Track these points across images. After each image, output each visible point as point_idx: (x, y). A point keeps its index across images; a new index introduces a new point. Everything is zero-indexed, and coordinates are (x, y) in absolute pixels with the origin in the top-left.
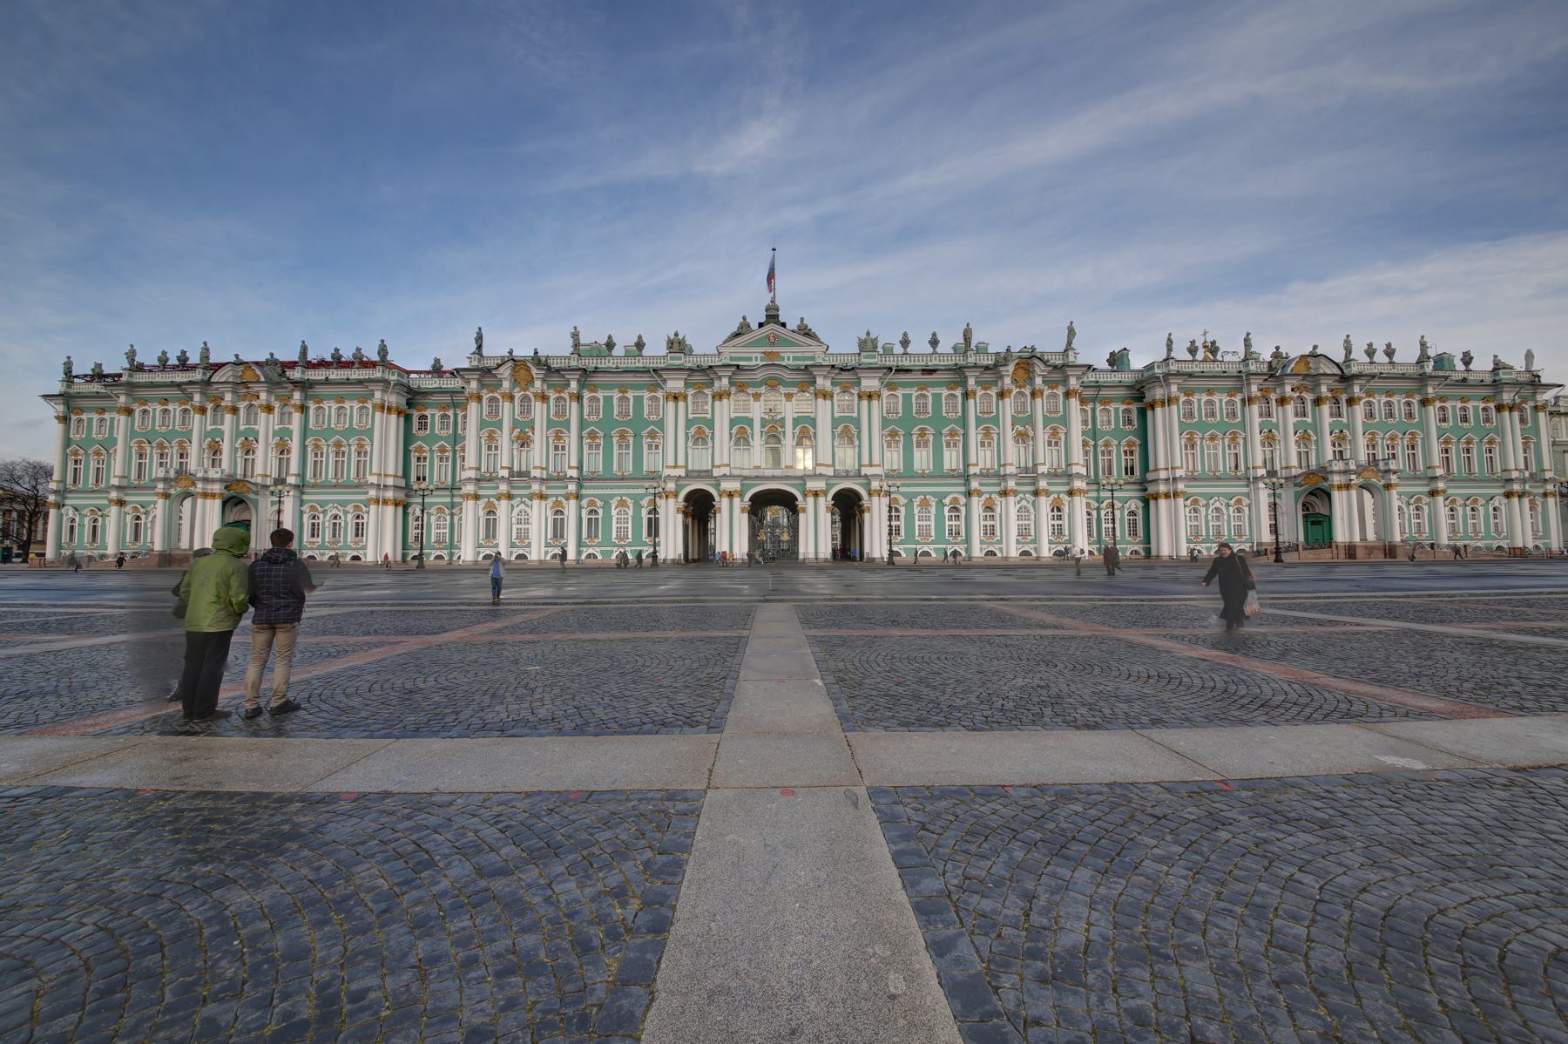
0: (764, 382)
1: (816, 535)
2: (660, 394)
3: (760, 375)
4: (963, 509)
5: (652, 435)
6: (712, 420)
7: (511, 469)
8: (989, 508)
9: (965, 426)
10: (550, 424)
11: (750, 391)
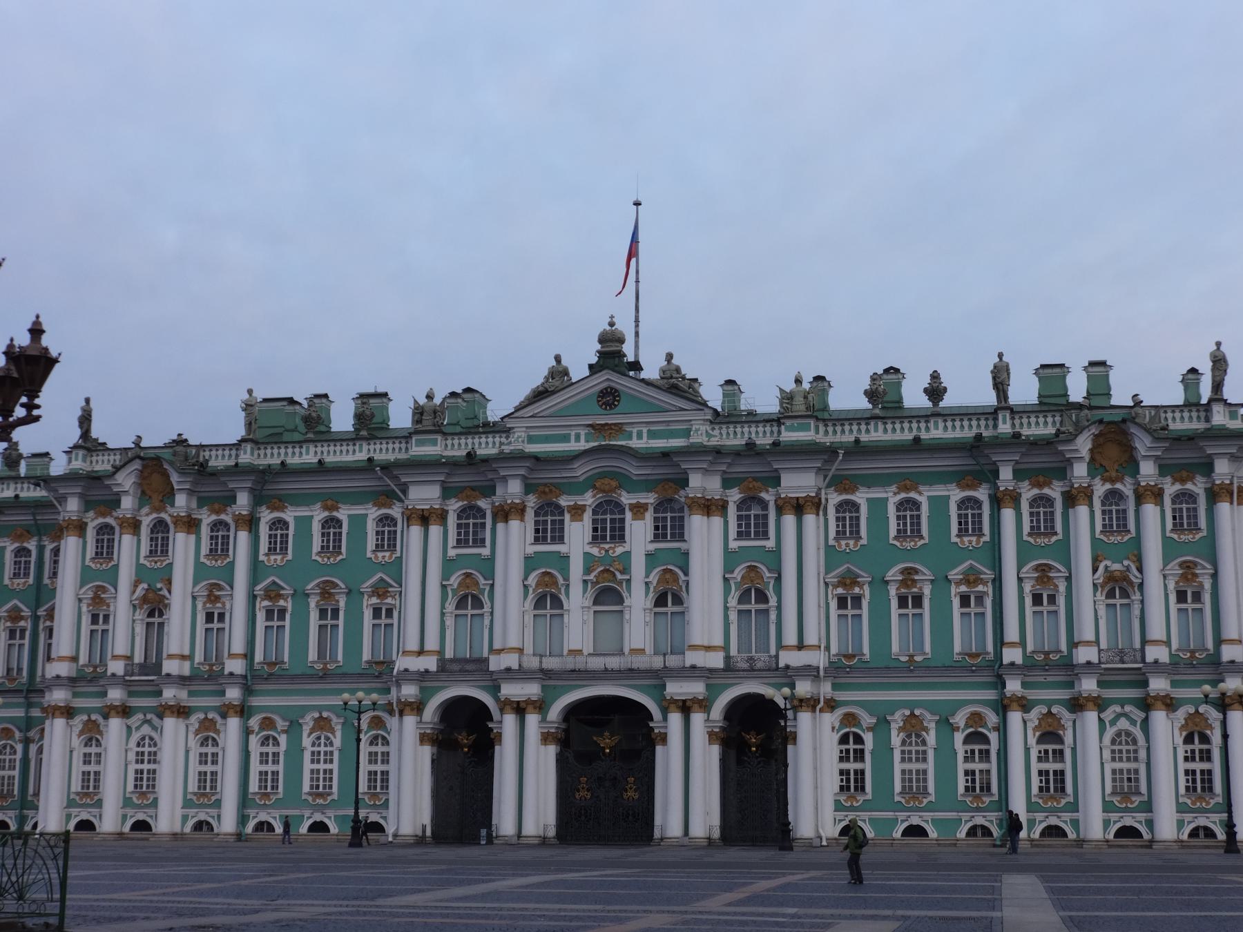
0: (591, 483)
1: (688, 787)
2: (396, 511)
3: (581, 471)
4: (993, 737)
5: (380, 590)
6: (491, 559)
7: (129, 658)
8: (1050, 734)
10: (200, 571)
11: (564, 501)
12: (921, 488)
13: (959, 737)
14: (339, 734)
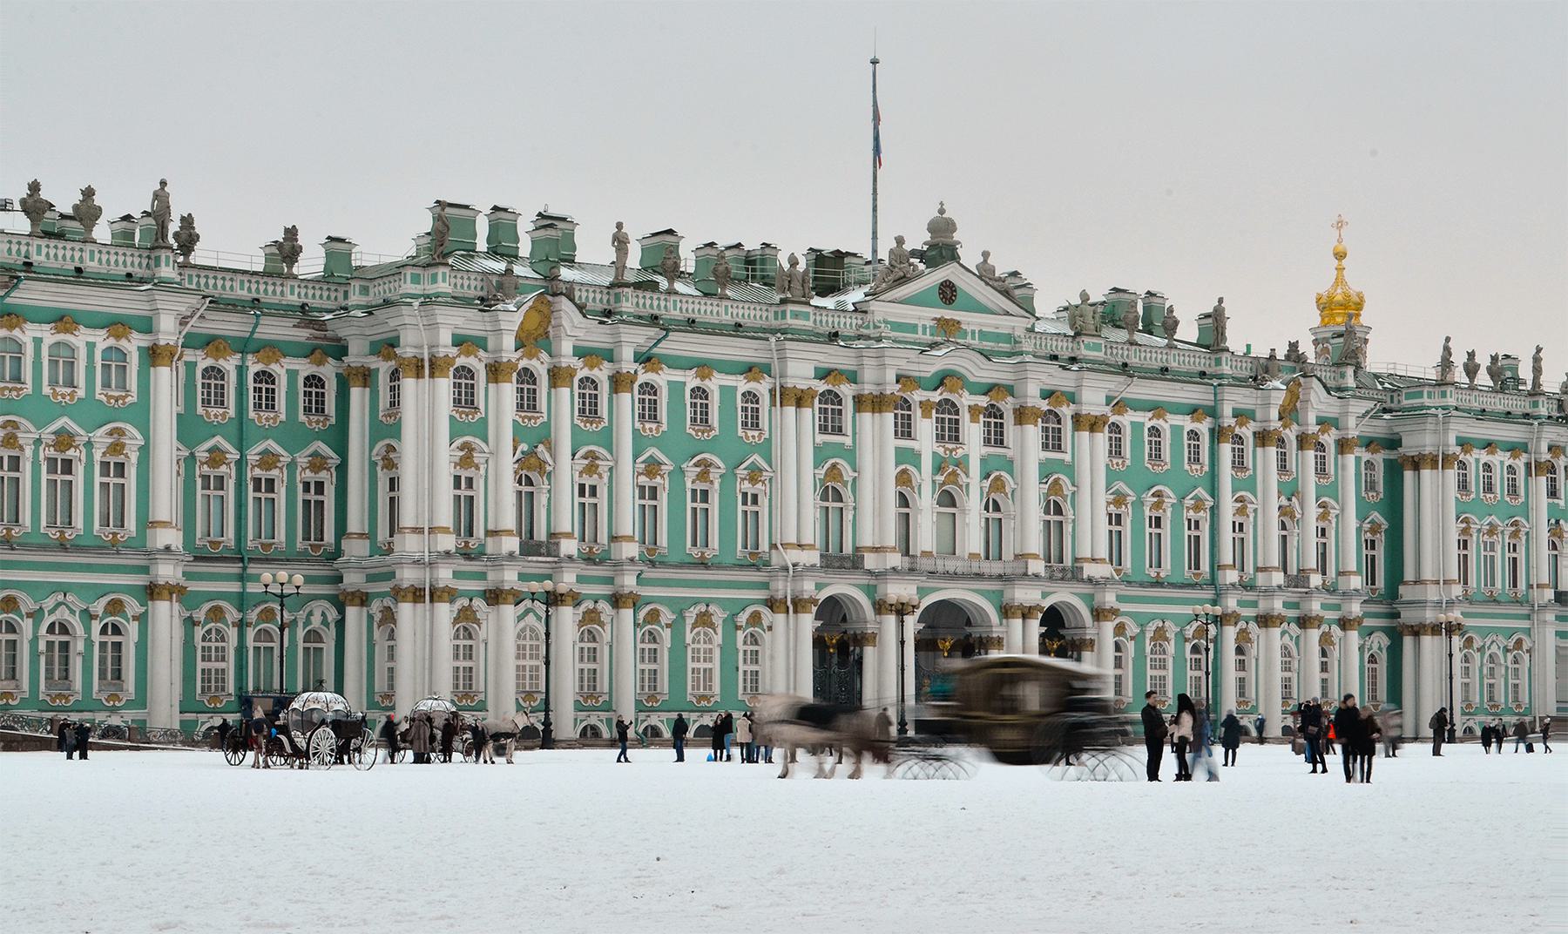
2: (762, 387)
9: (1214, 491)
11: (917, 396)
12: (1168, 416)
13: (1188, 646)
14: (720, 630)
